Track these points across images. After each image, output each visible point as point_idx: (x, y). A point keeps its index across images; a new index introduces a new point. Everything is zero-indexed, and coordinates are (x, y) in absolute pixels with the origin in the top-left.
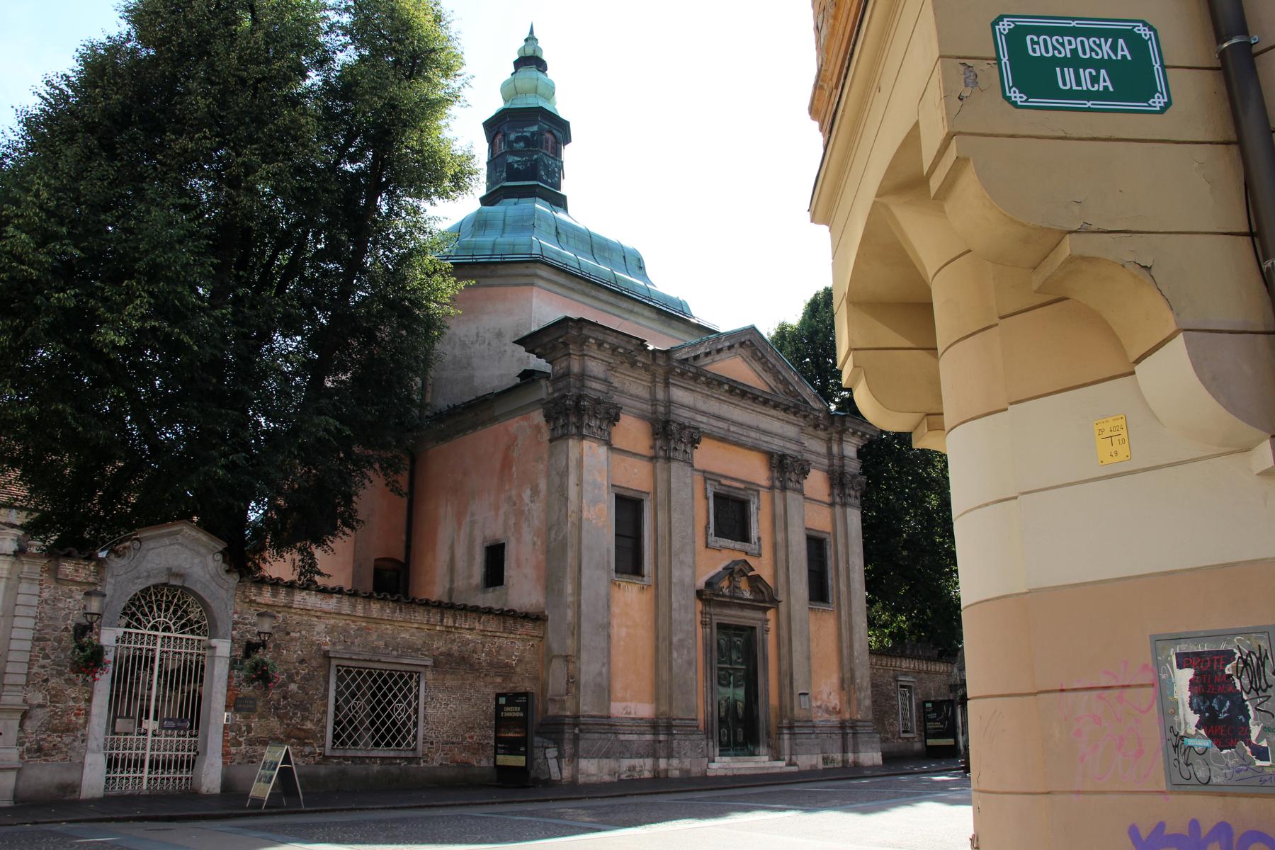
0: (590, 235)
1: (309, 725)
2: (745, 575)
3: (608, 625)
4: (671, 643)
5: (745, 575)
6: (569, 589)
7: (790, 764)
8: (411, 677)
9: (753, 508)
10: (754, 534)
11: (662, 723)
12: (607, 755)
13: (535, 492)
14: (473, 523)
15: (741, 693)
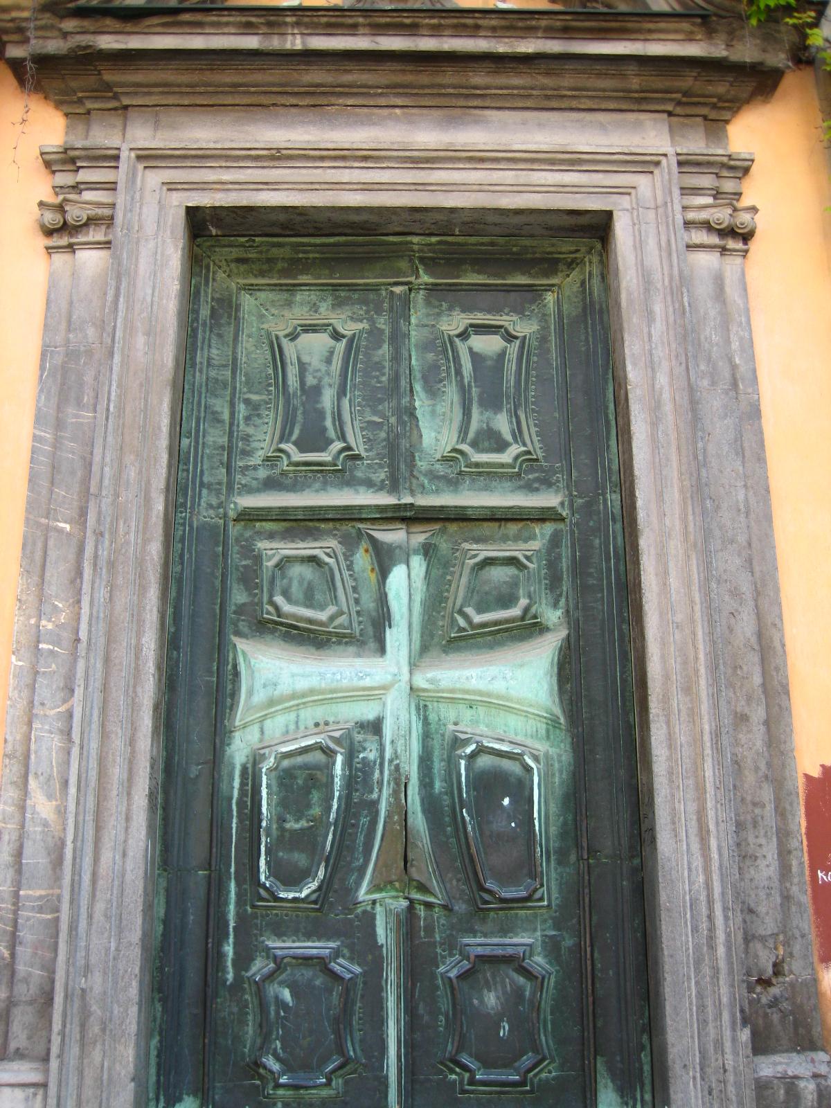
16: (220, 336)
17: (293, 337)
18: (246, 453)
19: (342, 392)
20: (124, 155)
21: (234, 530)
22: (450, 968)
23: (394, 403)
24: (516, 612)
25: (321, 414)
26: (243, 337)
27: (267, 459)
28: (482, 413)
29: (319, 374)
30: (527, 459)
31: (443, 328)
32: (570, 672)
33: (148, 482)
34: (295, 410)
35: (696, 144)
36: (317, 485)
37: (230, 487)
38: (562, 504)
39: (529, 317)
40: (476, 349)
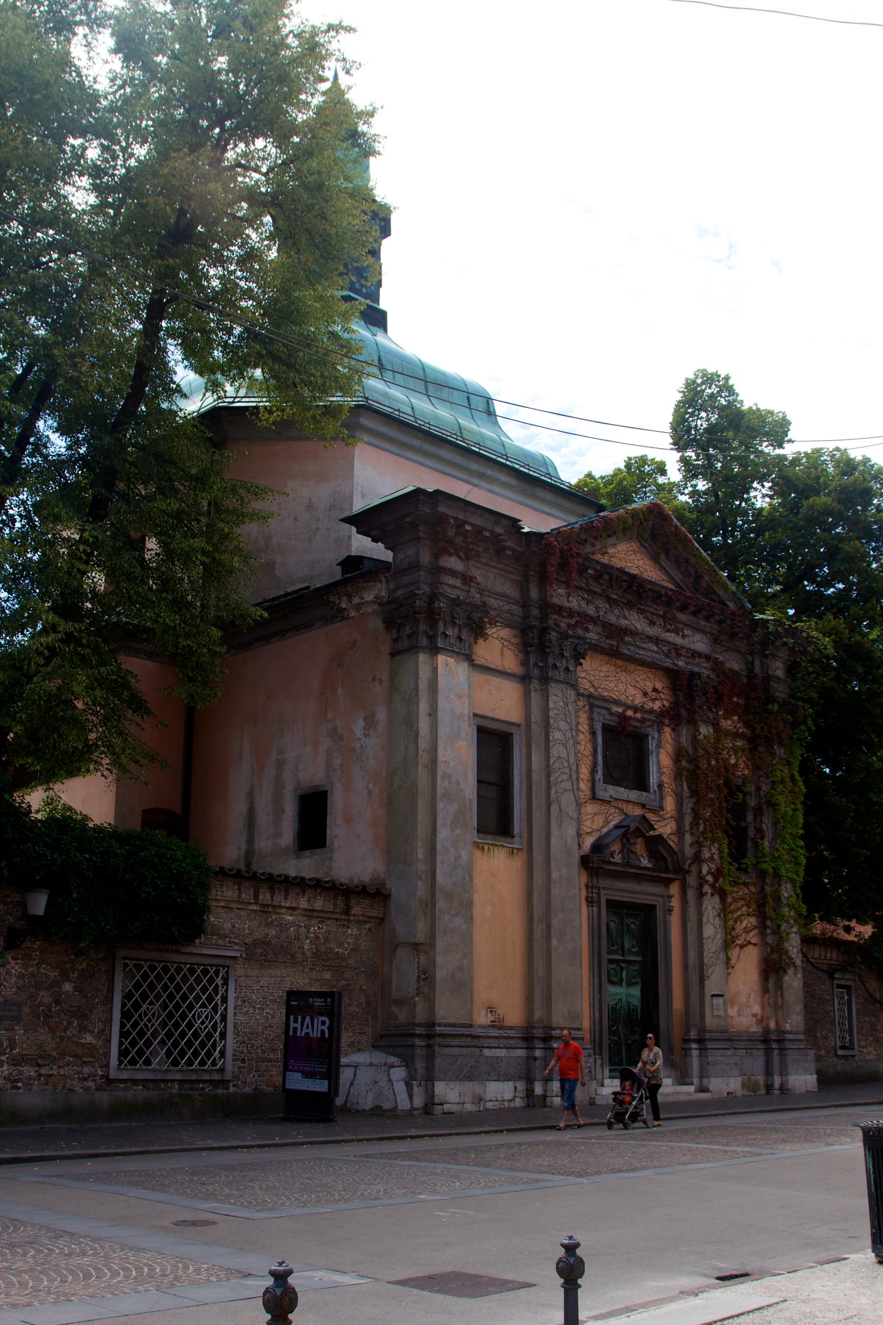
0: (424, 368)
1: (89, 1038)
2: (642, 835)
3: (470, 904)
4: (549, 926)
5: (642, 835)
6: (421, 854)
7: (702, 1089)
8: (217, 973)
9: (652, 745)
10: (653, 780)
11: (538, 1032)
12: (469, 1078)
13: (370, 722)
14: (281, 764)
15: (636, 991)
32: (642, 992)
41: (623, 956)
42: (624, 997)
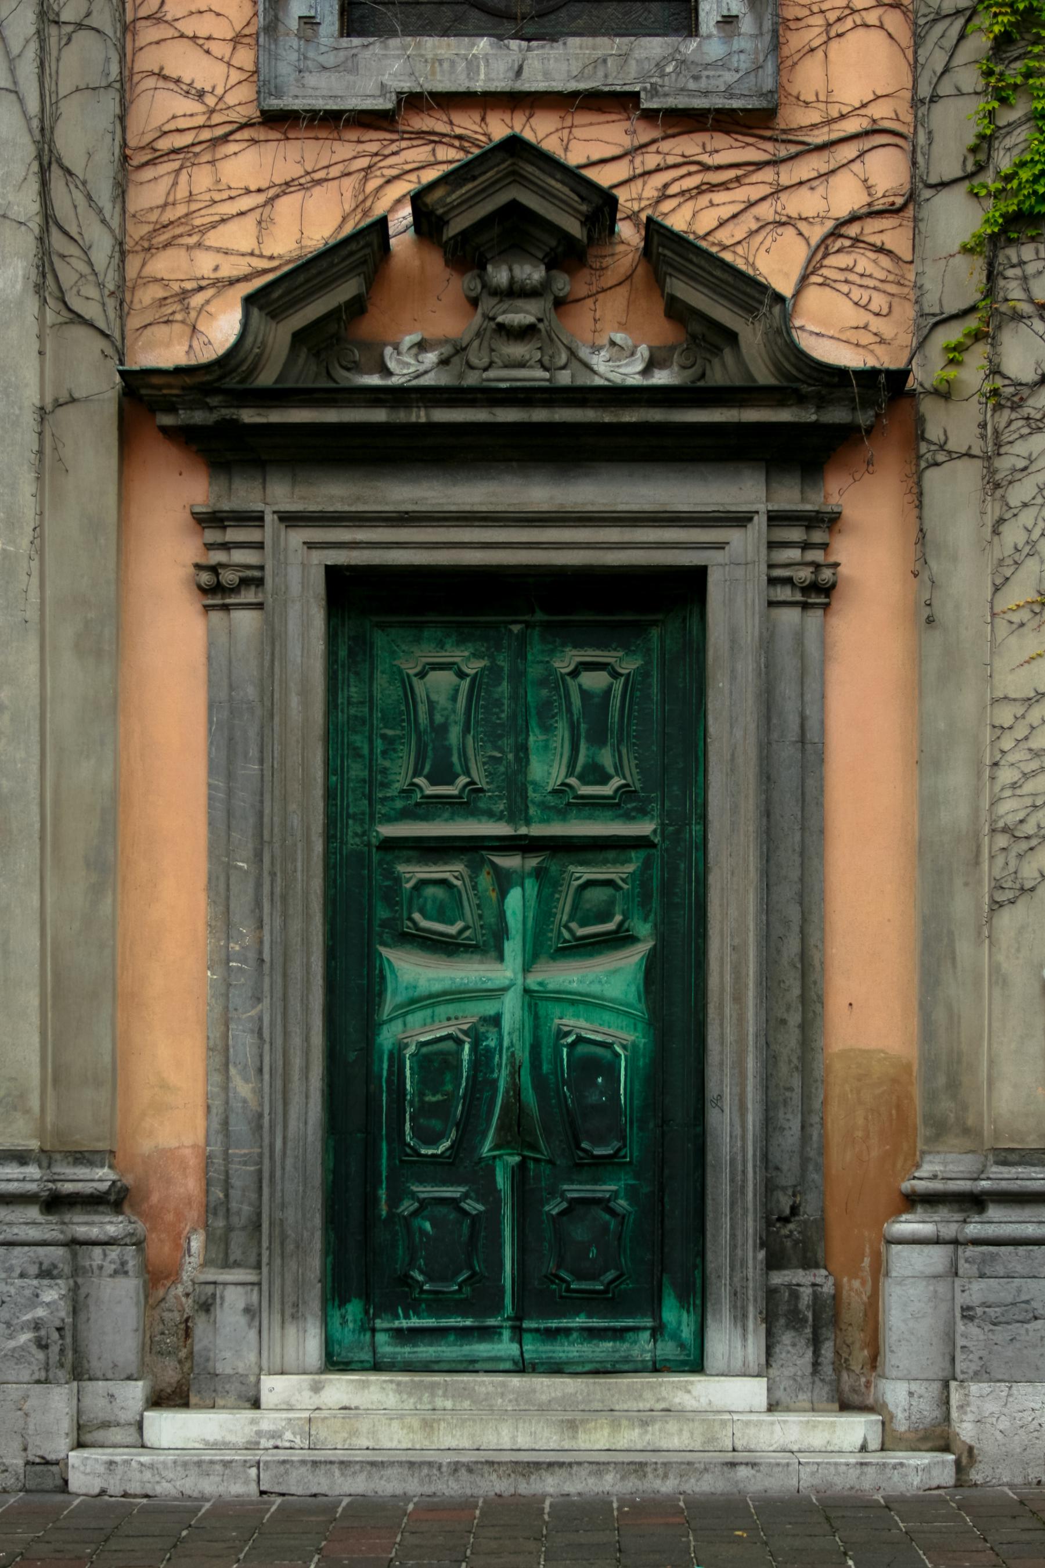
15: (614, 977)
16: (357, 674)
17: (422, 675)
18: (384, 785)
19: (466, 730)
20: (269, 518)
21: (376, 857)
22: (554, 1208)
23: (511, 741)
24: (611, 926)
25: (448, 750)
26: (378, 675)
27: (403, 791)
28: (588, 749)
29: (445, 713)
30: (626, 793)
31: (556, 665)
32: (656, 976)
33: (308, 828)
34: (426, 745)
35: (789, 497)
36: (446, 815)
37: (372, 817)
38: (655, 831)
39: (634, 652)
40: (585, 687)
41: (517, 813)
42: (511, 1008)
